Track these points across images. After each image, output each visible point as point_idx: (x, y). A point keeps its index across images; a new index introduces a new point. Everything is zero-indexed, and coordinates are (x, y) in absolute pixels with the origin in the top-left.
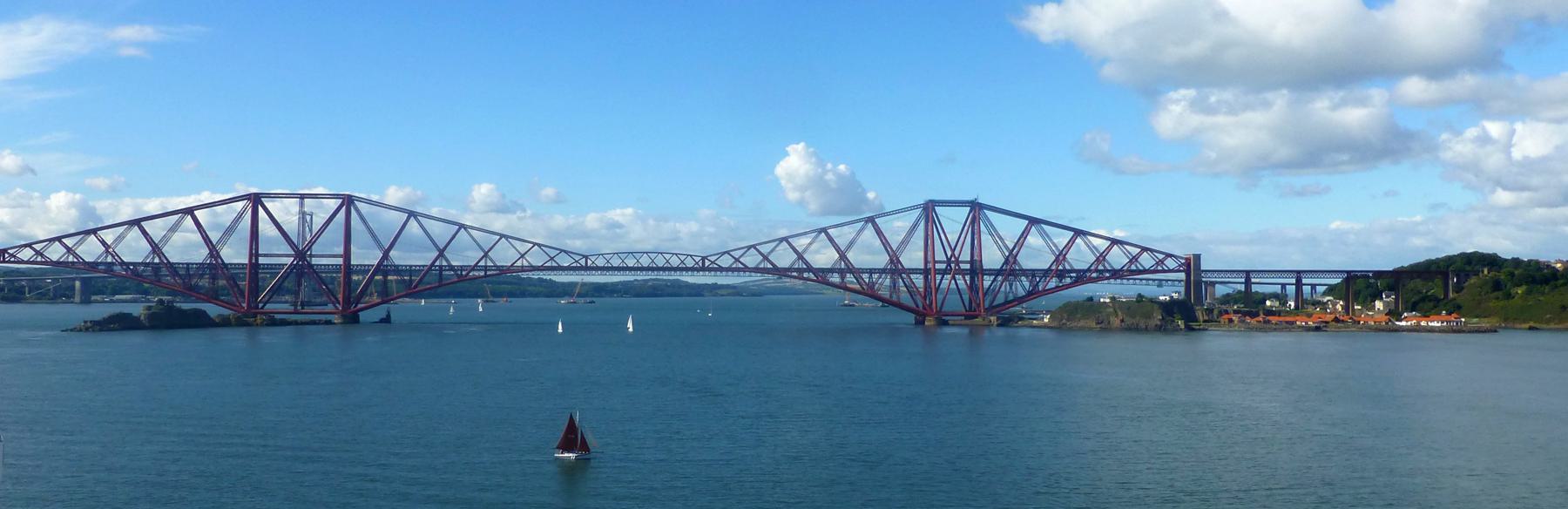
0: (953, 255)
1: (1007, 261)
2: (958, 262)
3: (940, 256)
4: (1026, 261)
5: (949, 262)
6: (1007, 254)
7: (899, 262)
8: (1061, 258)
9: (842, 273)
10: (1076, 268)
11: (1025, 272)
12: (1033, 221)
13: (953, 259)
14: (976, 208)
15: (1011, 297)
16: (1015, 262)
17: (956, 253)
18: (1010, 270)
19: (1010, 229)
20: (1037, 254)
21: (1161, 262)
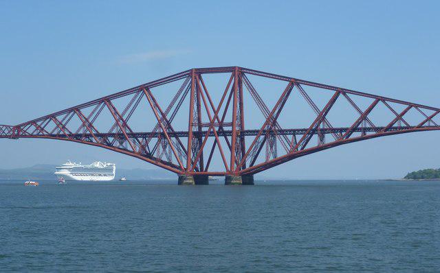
0: (216, 117)
1: (266, 123)
2: (221, 124)
3: (205, 119)
4: (284, 122)
5: (211, 125)
7: (169, 127)
9: (121, 137)
10: (335, 126)
11: (283, 132)
12: (294, 82)
13: (216, 121)
14: (239, 74)
15: (271, 158)
16: (275, 122)
17: (220, 115)
19: (271, 91)
20: (297, 115)
21: (429, 119)
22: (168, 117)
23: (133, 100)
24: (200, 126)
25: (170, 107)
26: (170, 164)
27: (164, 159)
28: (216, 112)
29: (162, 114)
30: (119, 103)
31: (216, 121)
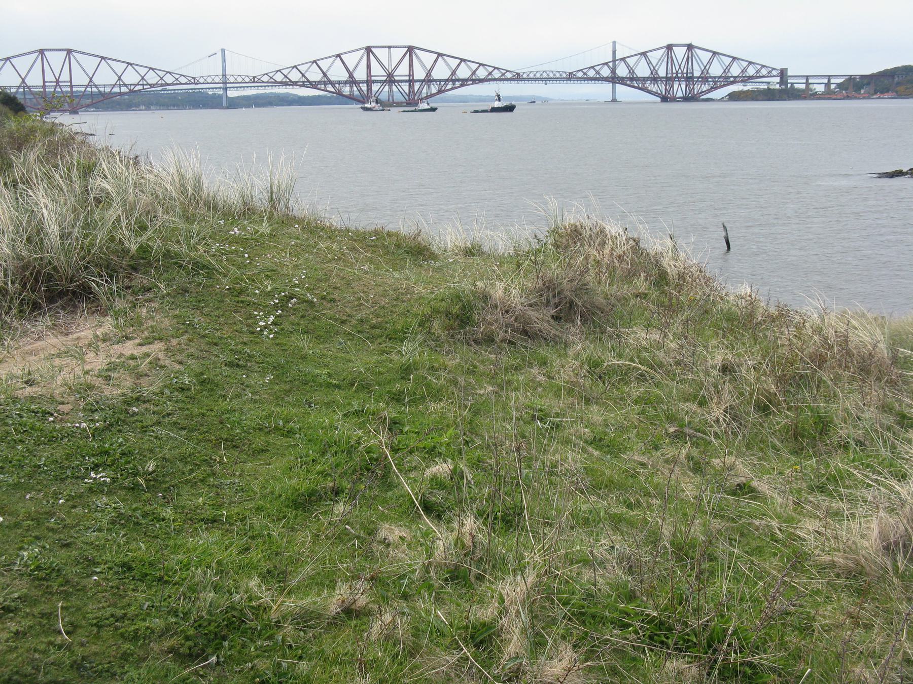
0: (680, 68)
1: (702, 73)
3: (674, 71)
5: (677, 73)
6: (703, 68)
7: (657, 73)
9: (632, 79)
14: (690, 47)
16: (708, 73)
19: (705, 57)
24: (672, 73)
26: (657, 93)
27: (654, 90)
28: (680, 66)
31: (680, 71)
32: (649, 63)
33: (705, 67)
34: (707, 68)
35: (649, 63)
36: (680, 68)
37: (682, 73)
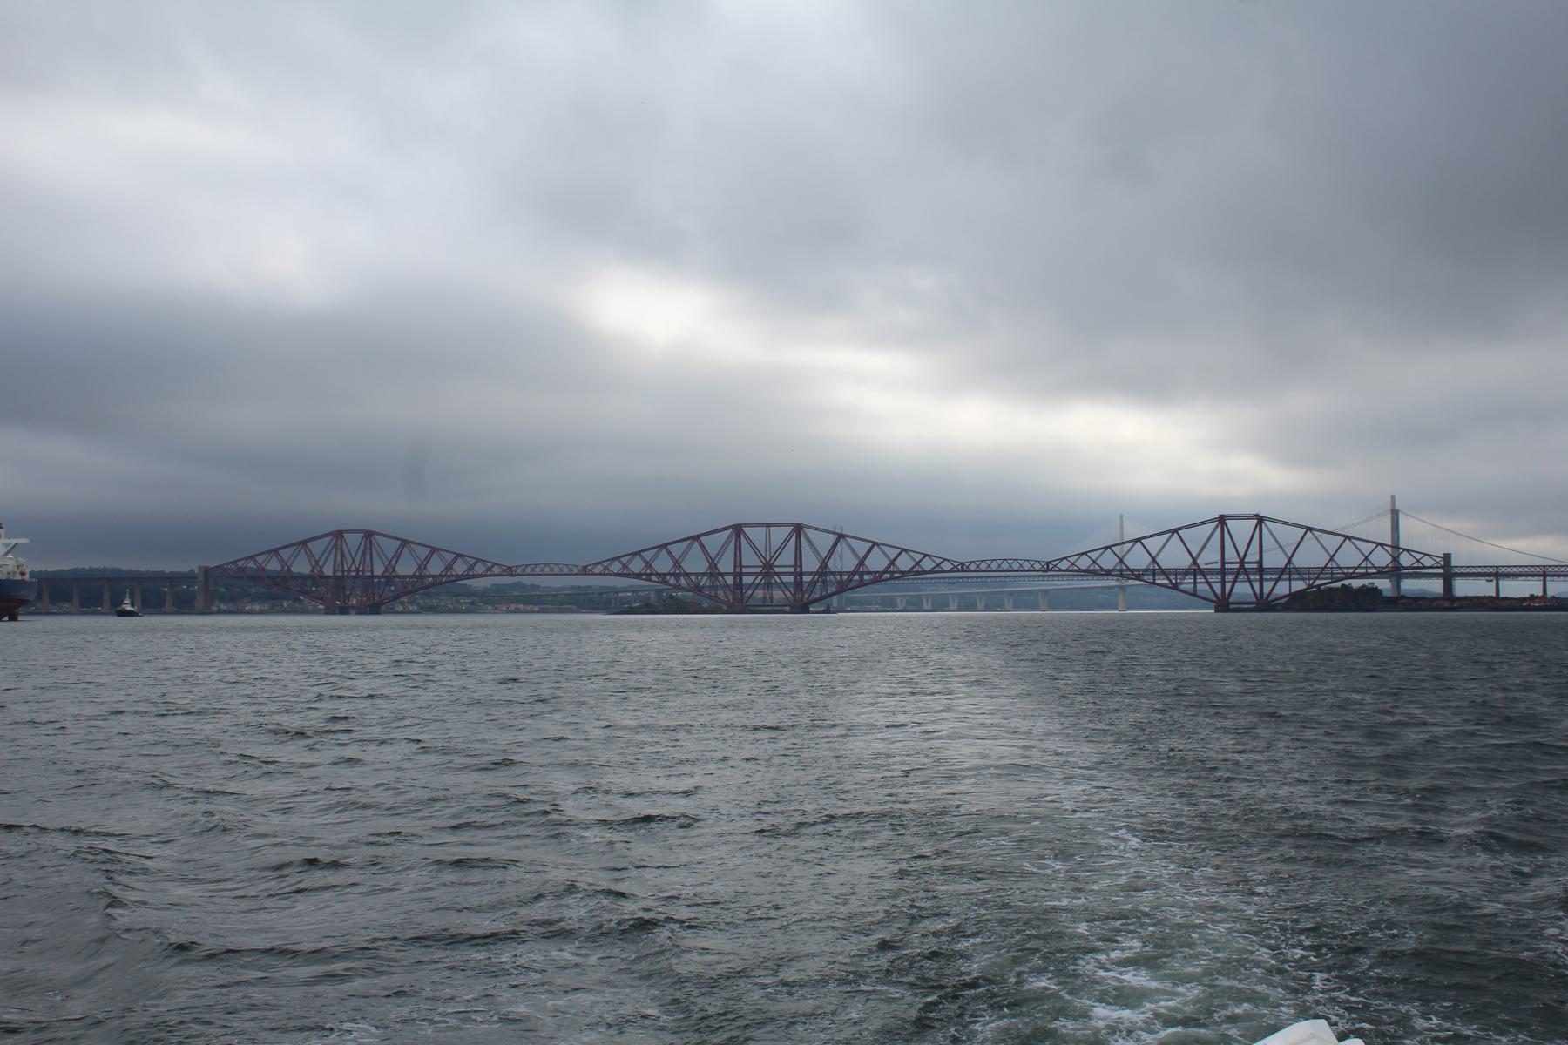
0: (353, 562)
3: (346, 568)
6: (387, 563)
7: (321, 571)
8: (422, 567)
13: (353, 568)
16: (394, 571)
17: (357, 561)
18: (389, 578)
22: (321, 563)
23: (294, 553)
24: (343, 571)
25: (321, 558)
28: (353, 559)
29: (316, 561)
30: (285, 554)
31: (353, 568)
32: (310, 556)
33: (390, 562)
34: (393, 562)
35: (310, 556)
36: (353, 562)
37: (357, 571)
